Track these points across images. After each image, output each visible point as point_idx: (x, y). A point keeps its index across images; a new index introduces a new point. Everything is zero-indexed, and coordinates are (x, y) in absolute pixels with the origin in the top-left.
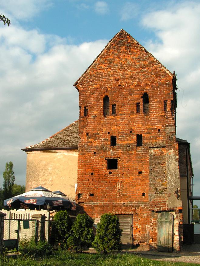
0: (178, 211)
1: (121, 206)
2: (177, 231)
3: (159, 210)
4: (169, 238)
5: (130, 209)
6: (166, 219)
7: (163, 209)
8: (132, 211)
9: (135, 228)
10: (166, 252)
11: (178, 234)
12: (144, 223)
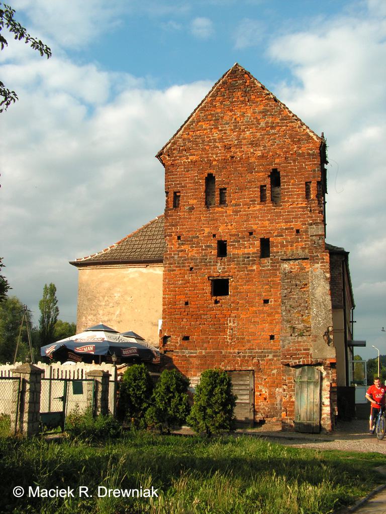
0: (330, 366)
1: (235, 356)
2: (327, 398)
4: (314, 410)
7: (303, 361)
8: (254, 365)
9: (257, 393)
10: (310, 433)
11: (329, 404)
12: (272, 385)
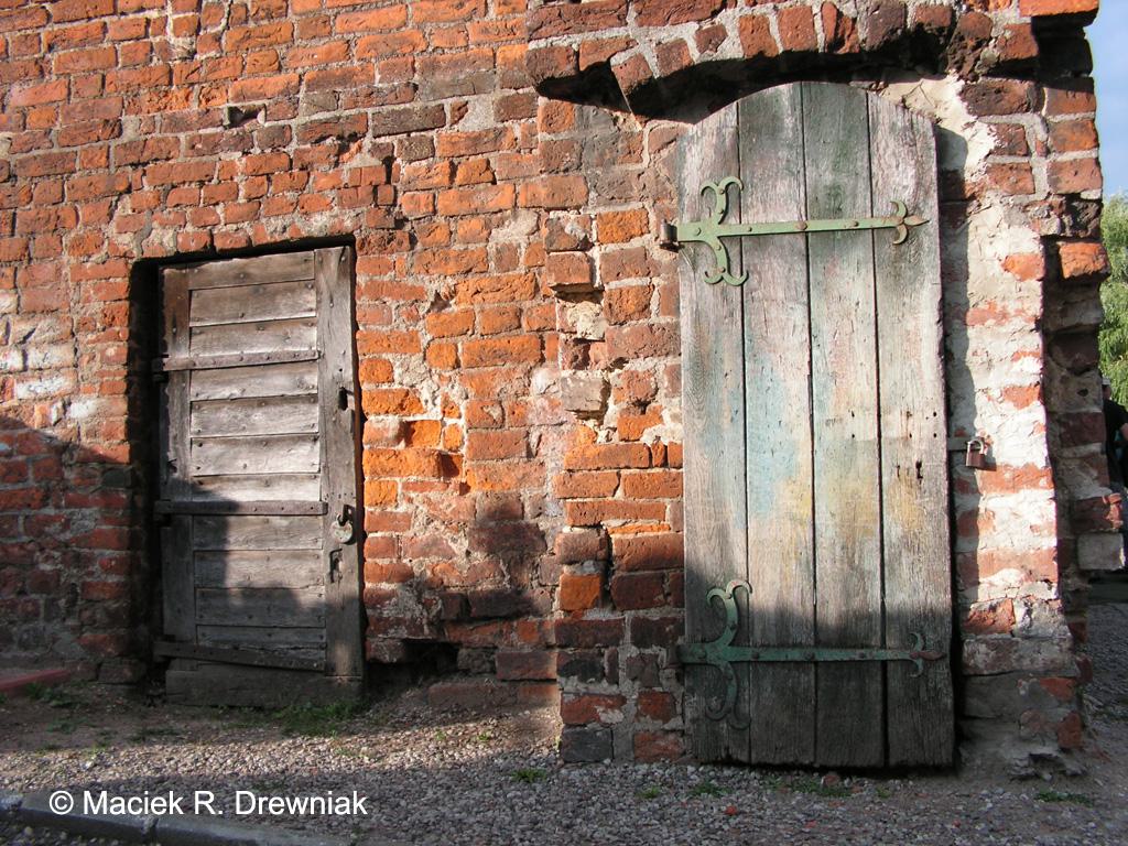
0: (1031, 49)
1: (213, 146)
2: (1012, 394)
3: (695, 55)
4: (894, 532)
5: (322, 177)
6: (833, 201)
7: (756, 26)
8: (347, 193)
9: (381, 424)
10: (845, 771)
11: (1038, 454)
12: (500, 342)
